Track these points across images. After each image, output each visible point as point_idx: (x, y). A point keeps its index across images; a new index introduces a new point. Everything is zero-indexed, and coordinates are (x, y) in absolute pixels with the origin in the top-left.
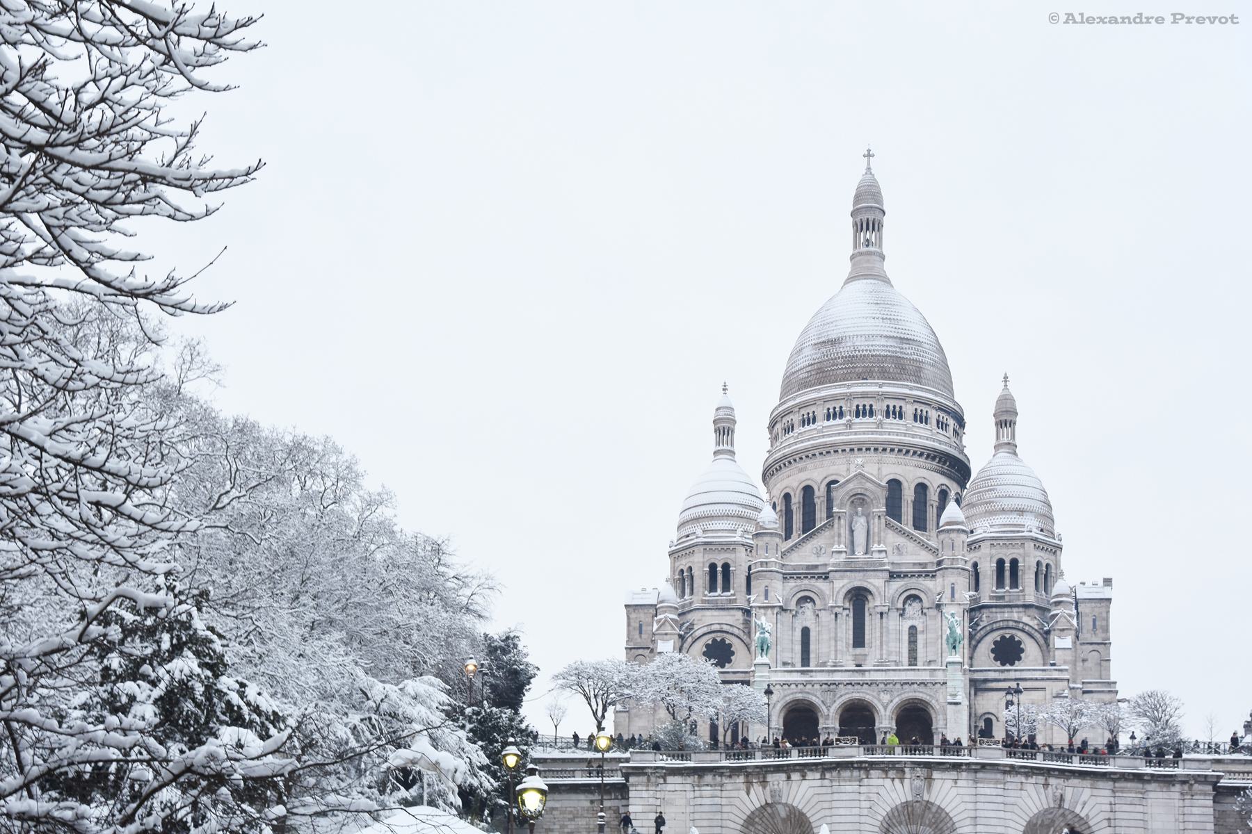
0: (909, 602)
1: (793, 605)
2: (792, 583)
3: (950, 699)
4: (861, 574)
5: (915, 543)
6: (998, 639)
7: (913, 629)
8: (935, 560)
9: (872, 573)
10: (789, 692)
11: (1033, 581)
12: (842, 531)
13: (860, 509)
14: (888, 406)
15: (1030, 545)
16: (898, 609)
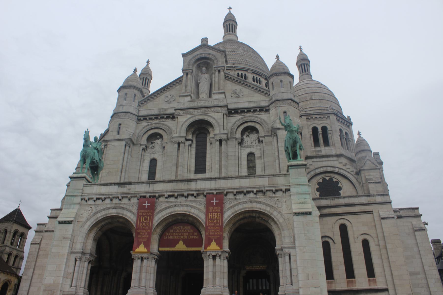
0: (247, 133)
1: (144, 141)
2: (144, 124)
3: (296, 208)
4: (203, 110)
5: (250, 88)
6: (321, 181)
7: (251, 155)
8: (268, 100)
9: (212, 109)
10: (102, 207)
11: (339, 140)
12: (189, 82)
13: (204, 69)
14: (238, 74)
15: (333, 118)
16: (236, 139)
